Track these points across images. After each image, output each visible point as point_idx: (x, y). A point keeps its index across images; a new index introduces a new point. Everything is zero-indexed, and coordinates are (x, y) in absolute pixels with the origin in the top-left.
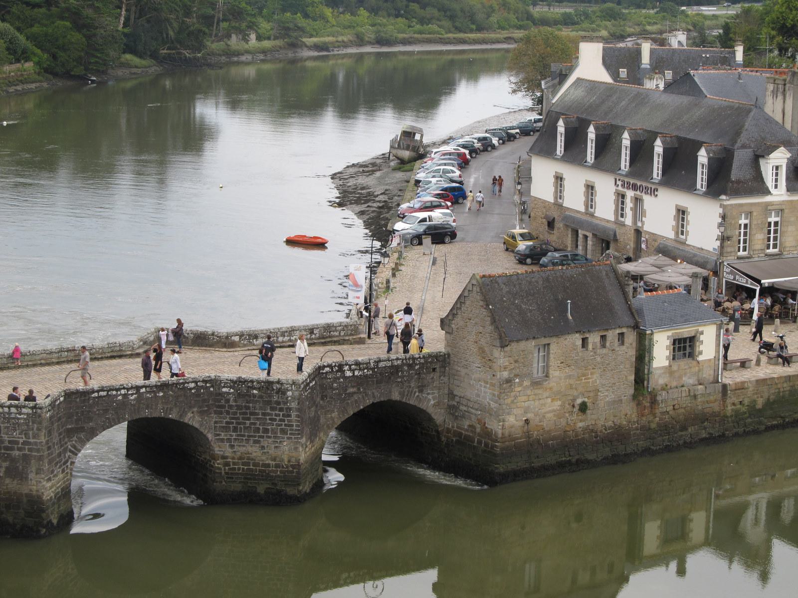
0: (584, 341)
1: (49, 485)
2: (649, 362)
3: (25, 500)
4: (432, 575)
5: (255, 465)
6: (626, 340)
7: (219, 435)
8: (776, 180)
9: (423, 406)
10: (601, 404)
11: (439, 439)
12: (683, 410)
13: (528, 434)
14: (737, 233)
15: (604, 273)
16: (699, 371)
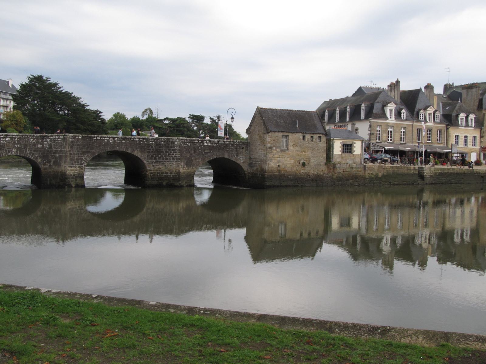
0: (304, 137)
1: (70, 169)
2: (332, 150)
3: (60, 174)
4: (243, 232)
5: (162, 173)
6: (322, 140)
7: (149, 161)
8: (391, 115)
9: (238, 162)
10: (312, 164)
11: (246, 177)
12: (347, 173)
13: (279, 171)
14: (376, 132)
15: (313, 115)
16: (354, 159)
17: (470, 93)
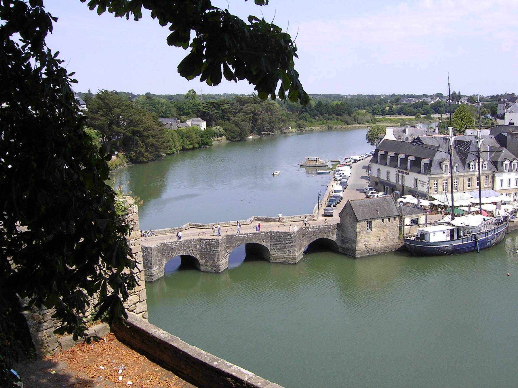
17: (514, 139)
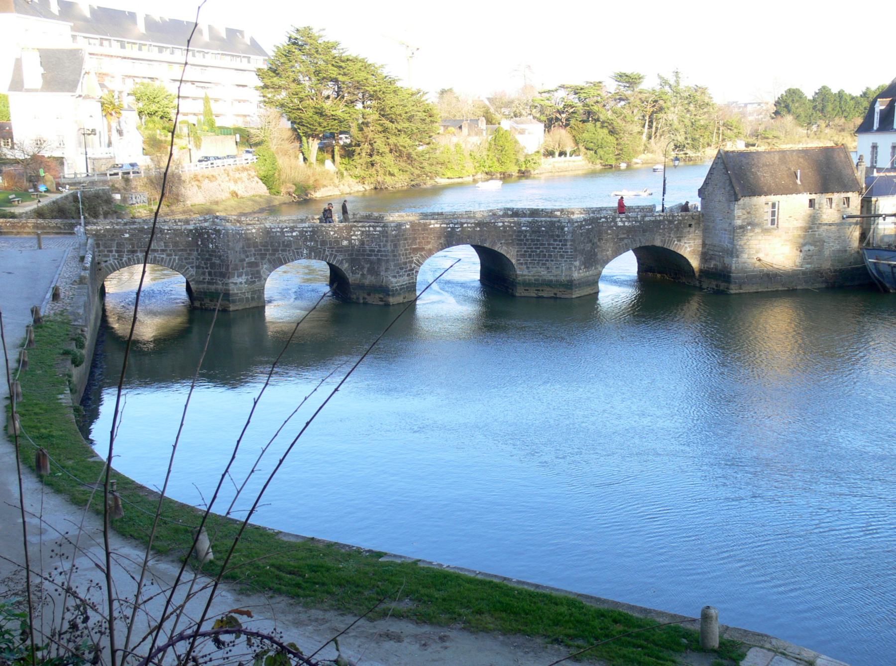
1: (394, 280)
9: (681, 252)
